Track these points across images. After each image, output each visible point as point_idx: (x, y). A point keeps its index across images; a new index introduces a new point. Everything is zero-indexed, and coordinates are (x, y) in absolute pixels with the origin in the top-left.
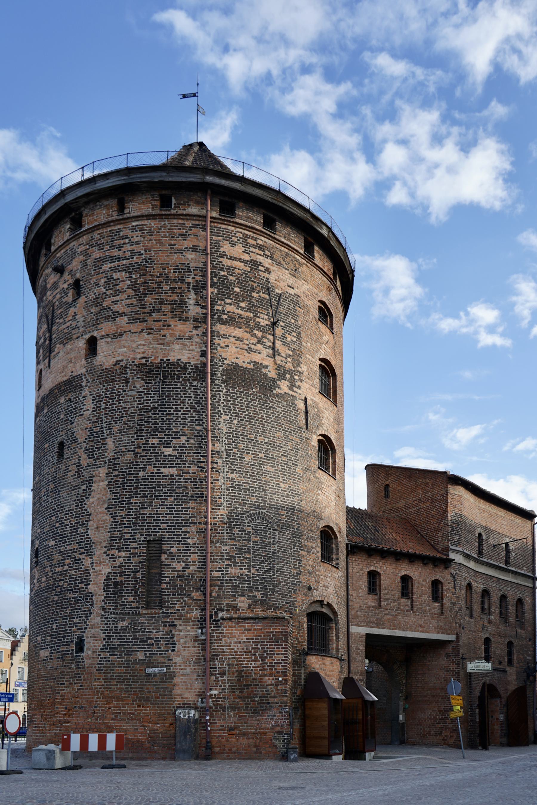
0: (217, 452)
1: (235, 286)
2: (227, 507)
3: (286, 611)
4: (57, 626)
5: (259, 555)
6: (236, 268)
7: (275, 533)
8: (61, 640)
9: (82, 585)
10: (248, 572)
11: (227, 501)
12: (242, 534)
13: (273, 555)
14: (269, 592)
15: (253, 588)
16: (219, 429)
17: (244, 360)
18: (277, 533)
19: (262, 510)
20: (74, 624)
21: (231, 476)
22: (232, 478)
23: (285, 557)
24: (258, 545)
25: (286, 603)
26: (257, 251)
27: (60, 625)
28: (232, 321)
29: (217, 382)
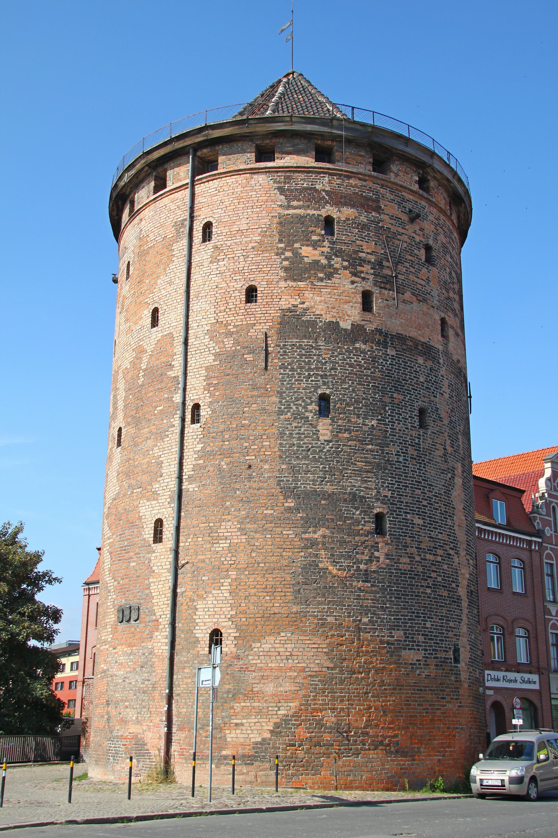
4: (432, 625)
8: (438, 644)
9: (454, 585)
20: (450, 627)
27: (437, 626)
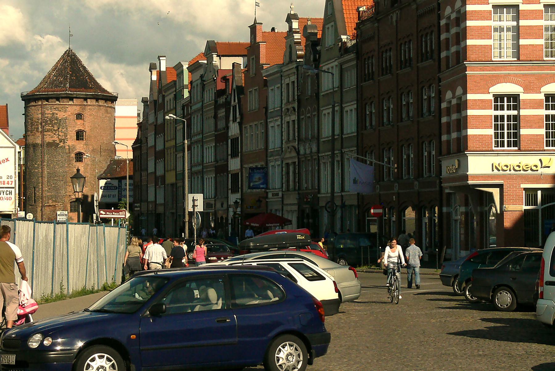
17: (51, 141)
28: (48, 131)
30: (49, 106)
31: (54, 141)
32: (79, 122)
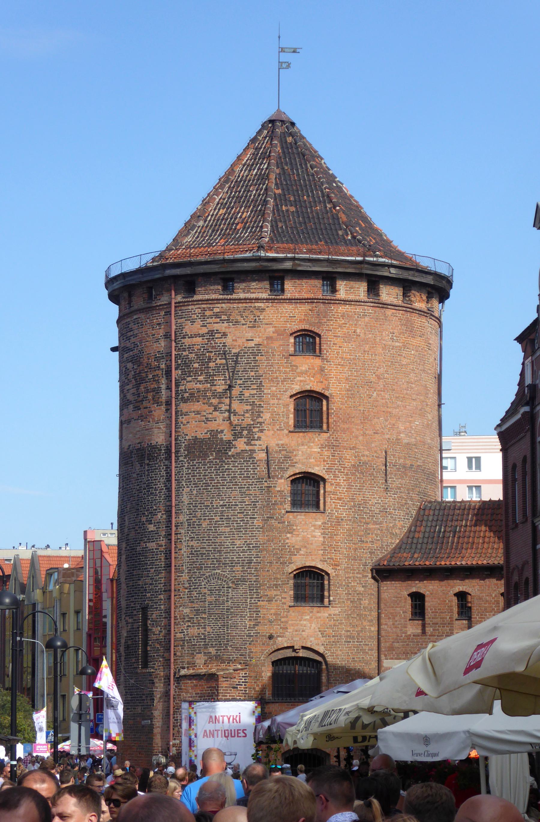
0: (181, 523)
1: (194, 363)
2: (188, 573)
3: (241, 663)
5: (213, 614)
6: (195, 345)
7: (228, 590)
10: (204, 631)
11: (188, 567)
12: (199, 596)
13: (227, 612)
14: (223, 647)
15: (208, 645)
16: (182, 502)
18: (230, 590)
19: (217, 571)
21: (192, 543)
22: (192, 546)
23: (239, 612)
24: (212, 604)
25: (240, 655)
26: (214, 320)
28: (193, 397)
29: (181, 459)
30: (195, 309)
31: (214, 433)
32: (306, 363)
